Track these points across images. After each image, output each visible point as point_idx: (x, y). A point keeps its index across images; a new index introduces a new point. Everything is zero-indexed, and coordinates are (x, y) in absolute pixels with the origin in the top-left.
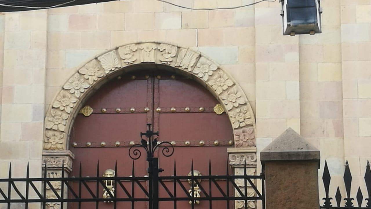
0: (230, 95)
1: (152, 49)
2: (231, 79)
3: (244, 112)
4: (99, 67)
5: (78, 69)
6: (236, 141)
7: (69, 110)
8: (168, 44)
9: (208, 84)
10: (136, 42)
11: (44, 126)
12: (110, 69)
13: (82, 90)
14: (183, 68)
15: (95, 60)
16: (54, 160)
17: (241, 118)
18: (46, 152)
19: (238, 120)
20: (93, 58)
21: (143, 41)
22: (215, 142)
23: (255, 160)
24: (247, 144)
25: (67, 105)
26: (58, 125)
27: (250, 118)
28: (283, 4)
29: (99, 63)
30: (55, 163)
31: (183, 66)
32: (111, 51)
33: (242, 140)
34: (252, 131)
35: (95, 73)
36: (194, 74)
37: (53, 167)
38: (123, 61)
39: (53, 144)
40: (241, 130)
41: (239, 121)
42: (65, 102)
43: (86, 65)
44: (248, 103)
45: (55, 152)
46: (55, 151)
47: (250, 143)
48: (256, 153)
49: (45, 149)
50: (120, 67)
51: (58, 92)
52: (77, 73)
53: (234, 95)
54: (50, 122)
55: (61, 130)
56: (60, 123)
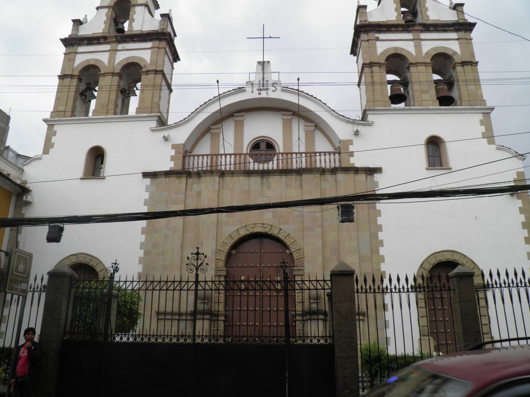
7: (226, 251)
10: (254, 223)
13: (231, 243)
21: (257, 223)
28: (339, 210)
32: (243, 227)
40: (298, 260)
48: (304, 270)
49: (216, 267)
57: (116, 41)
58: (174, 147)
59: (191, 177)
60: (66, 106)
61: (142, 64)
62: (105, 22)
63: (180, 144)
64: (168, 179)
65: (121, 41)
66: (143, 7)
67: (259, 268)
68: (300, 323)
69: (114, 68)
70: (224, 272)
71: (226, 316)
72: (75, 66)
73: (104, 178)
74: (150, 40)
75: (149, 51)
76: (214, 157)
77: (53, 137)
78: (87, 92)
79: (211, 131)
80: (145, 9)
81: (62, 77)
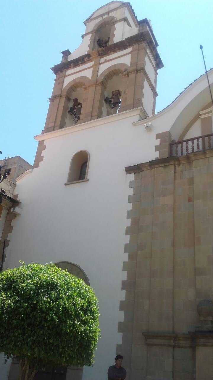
57: (98, 56)
58: (158, 136)
59: (179, 164)
60: (55, 122)
61: (123, 69)
62: (89, 46)
63: (166, 132)
64: (153, 170)
65: (103, 55)
66: (123, 22)
69: (97, 79)
72: (63, 88)
73: (88, 181)
74: (130, 46)
75: (130, 56)
76: (207, 139)
77: (43, 152)
78: (75, 109)
79: (201, 117)
80: (124, 23)
81: (51, 100)
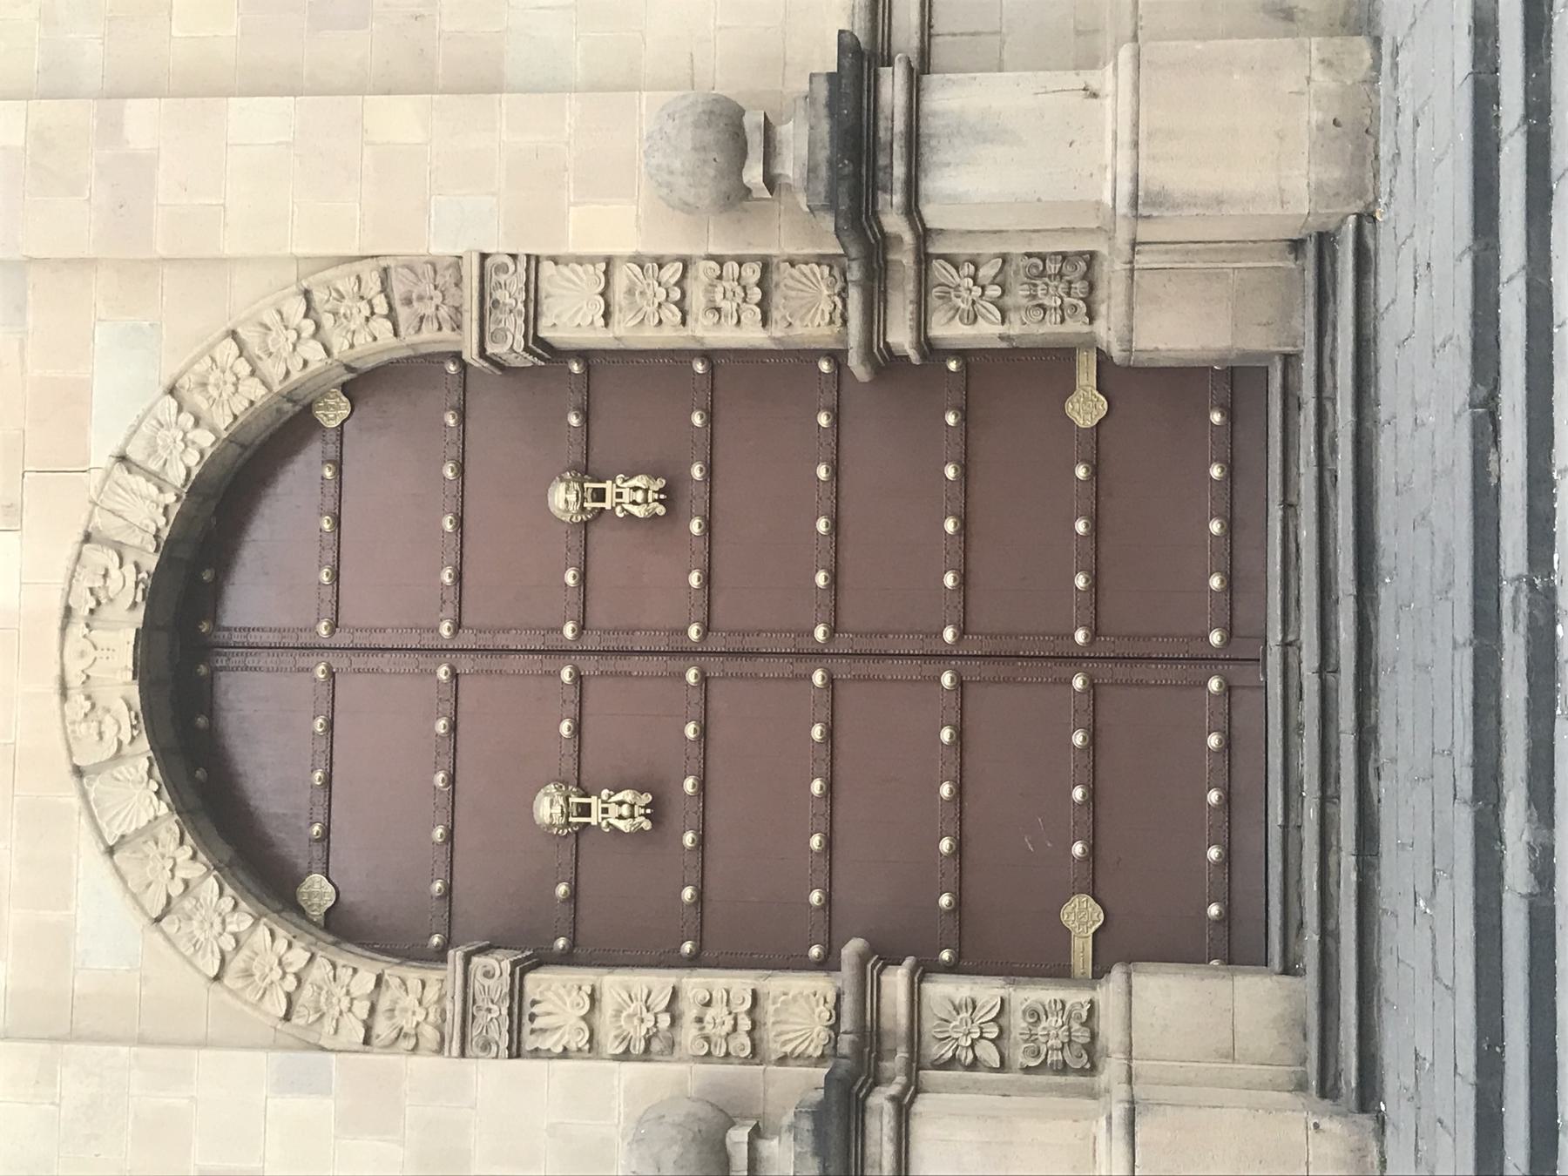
0: (272, 350)
1: (85, 636)
2: (212, 346)
3: (334, 299)
4: (143, 839)
5: (146, 921)
6: (440, 329)
7: (298, 957)
8: (73, 576)
9: (226, 429)
10: (56, 698)
11: (357, 1052)
12: (155, 798)
13: (227, 903)
14: (162, 521)
15: (115, 857)
16: (483, 1012)
17: (355, 311)
18: (451, 1042)
19: (363, 321)
20: (109, 863)
21: (56, 671)
22: (451, 421)
23: (509, 261)
24: (453, 290)
25: (280, 963)
26: (352, 1000)
27: (359, 278)
29: (129, 842)
30: (495, 1008)
31: (155, 522)
32: (84, 795)
33: (437, 308)
34: (406, 271)
35: (163, 856)
36: (189, 484)
37: (510, 1014)
38: (126, 749)
39: (423, 1017)
40: (403, 312)
41: (367, 319)
42: (267, 970)
43: (135, 890)
44: (305, 284)
45: (454, 1009)
46: (449, 1006)
47: (446, 278)
48: (484, 257)
49: (440, 1050)
50: (149, 758)
51: (226, 996)
52: (163, 923)
53: (274, 334)
54: (342, 1031)
55: (371, 985)
56: (344, 990)
67: (465, 664)
68: (945, 297)
70: (488, 974)
71: (883, 954)
